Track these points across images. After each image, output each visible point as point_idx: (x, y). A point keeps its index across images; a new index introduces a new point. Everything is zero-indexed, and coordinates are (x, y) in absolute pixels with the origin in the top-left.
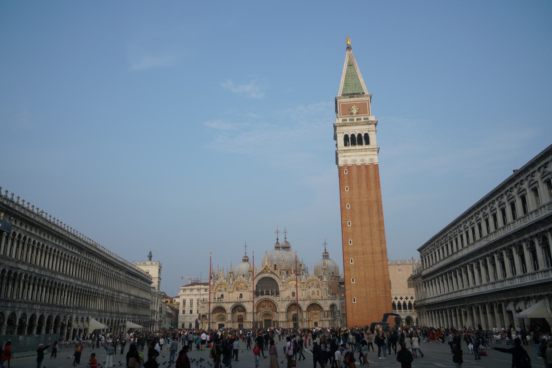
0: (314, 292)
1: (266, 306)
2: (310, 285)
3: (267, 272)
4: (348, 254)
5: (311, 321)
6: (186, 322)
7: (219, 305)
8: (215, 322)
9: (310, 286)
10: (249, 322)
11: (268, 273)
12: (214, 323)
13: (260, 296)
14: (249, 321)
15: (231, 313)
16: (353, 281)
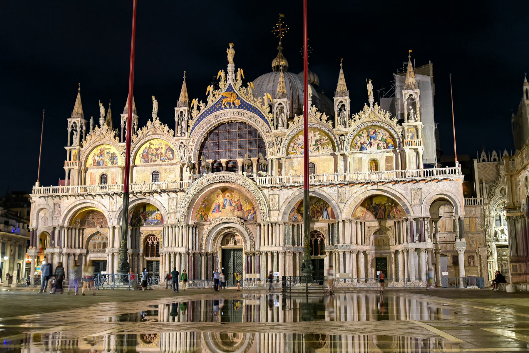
1: (224, 206)
9: (362, 144)
11: (235, 107)
13: (205, 175)
14: (170, 250)
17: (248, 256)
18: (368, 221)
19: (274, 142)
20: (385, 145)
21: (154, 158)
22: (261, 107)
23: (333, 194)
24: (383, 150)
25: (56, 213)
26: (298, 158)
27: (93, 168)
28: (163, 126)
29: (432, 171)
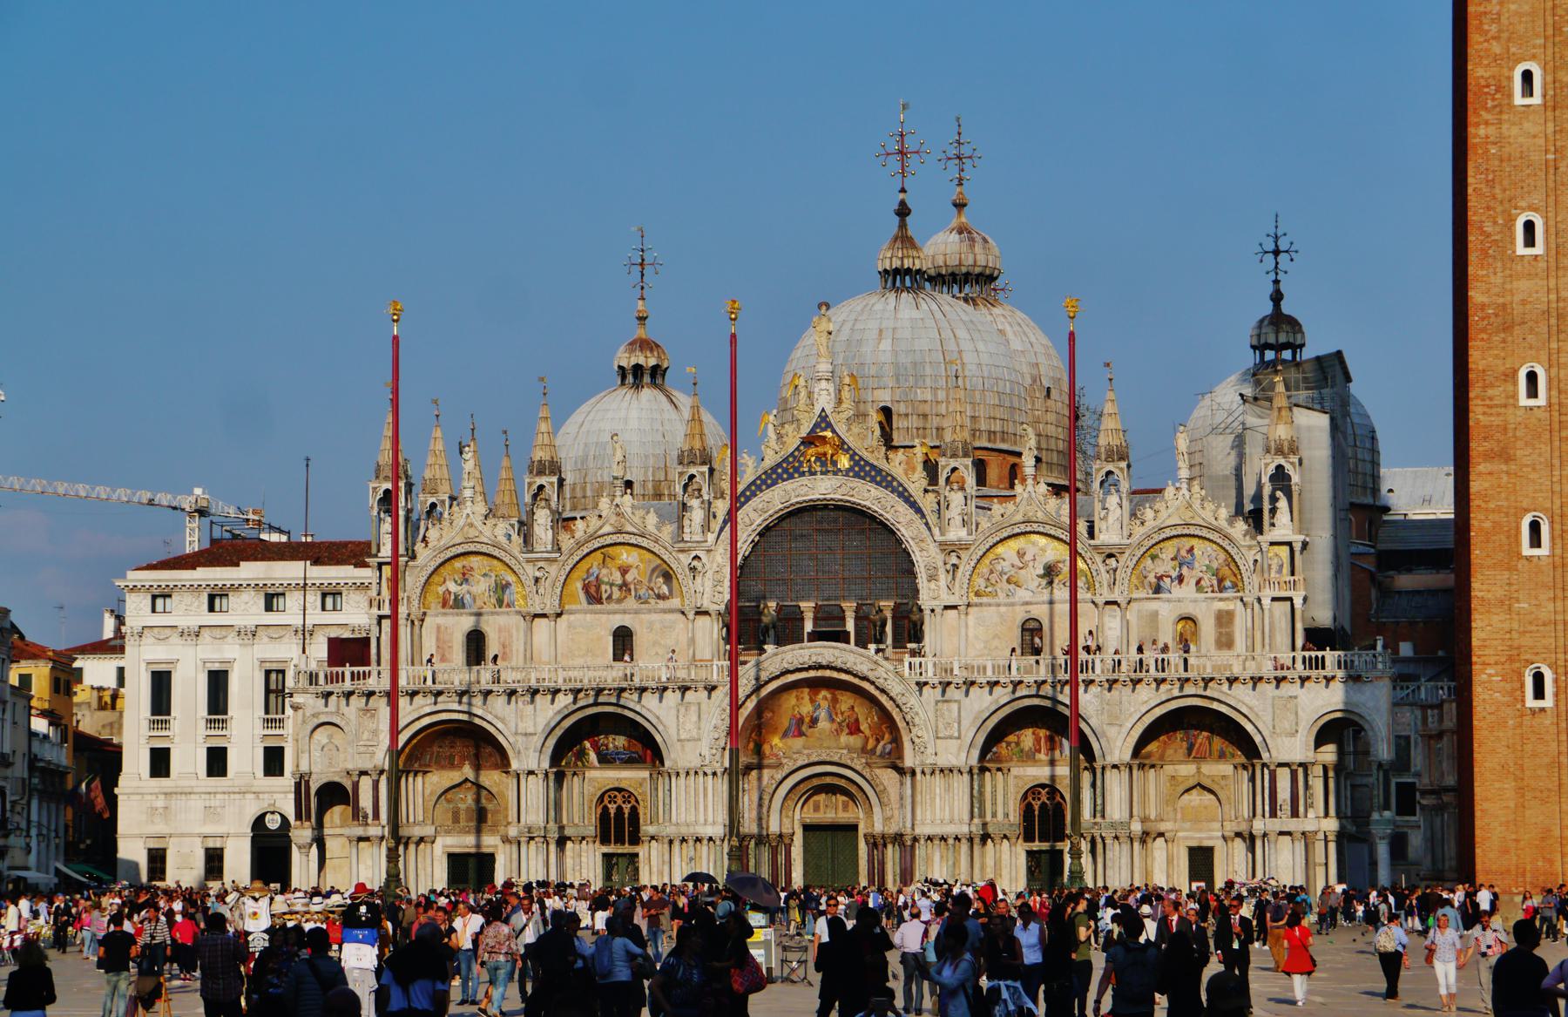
0: (1188, 618)
1: (814, 721)
2: (1165, 566)
3: (827, 465)
4: (1507, 328)
5: (1160, 841)
6: (182, 835)
7: (452, 709)
8: (422, 839)
9: (1160, 578)
10: (684, 840)
12: (412, 847)
13: (770, 648)
14: (684, 831)
15: (546, 775)
16: (1536, 541)
17: (875, 845)
18: (1172, 763)
19: (940, 564)
20: (1215, 582)
21: (616, 594)
22: (906, 474)
23: (1091, 703)
24: (1210, 595)
25: (365, 736)
26: (998, 605)
27: (445, 614)
28: (641, 512)
29: (1323, 657)
